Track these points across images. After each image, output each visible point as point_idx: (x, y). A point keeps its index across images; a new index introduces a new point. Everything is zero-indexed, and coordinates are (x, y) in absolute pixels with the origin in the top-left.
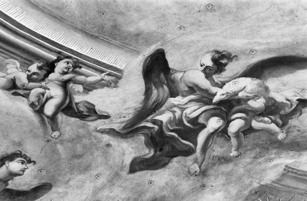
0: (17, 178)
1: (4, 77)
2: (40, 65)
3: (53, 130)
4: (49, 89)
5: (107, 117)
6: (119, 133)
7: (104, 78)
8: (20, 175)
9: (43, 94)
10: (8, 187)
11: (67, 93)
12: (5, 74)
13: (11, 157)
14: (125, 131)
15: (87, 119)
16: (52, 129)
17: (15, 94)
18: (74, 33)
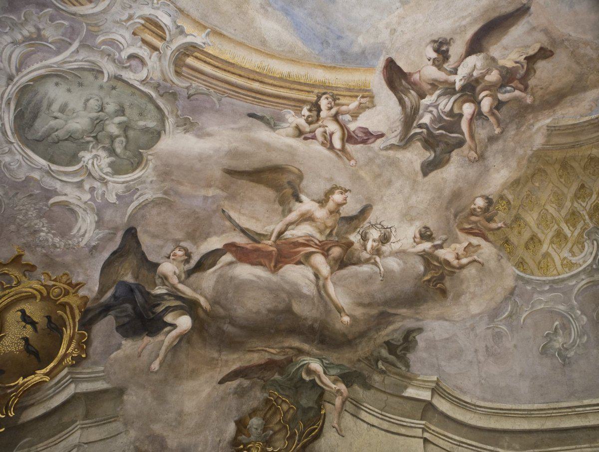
0: (344, 206)
1: (289, 127)
2: (308, 107)
3: (350, 160)
4: (327, 126)
5: (382, 135)
6: (399, 146)
7: (361, 102)
8: (345, 204)
9: (325, 132)
10: (342, 215)
11: (343, 127)
12: (288, 125)
13: (331, 191)
14: (403, 143)
15: (369, 142)
16: (348, 159)
17: (306, 139)
18: (316, 70)
